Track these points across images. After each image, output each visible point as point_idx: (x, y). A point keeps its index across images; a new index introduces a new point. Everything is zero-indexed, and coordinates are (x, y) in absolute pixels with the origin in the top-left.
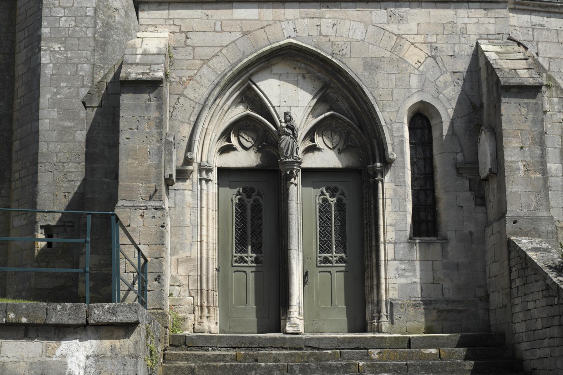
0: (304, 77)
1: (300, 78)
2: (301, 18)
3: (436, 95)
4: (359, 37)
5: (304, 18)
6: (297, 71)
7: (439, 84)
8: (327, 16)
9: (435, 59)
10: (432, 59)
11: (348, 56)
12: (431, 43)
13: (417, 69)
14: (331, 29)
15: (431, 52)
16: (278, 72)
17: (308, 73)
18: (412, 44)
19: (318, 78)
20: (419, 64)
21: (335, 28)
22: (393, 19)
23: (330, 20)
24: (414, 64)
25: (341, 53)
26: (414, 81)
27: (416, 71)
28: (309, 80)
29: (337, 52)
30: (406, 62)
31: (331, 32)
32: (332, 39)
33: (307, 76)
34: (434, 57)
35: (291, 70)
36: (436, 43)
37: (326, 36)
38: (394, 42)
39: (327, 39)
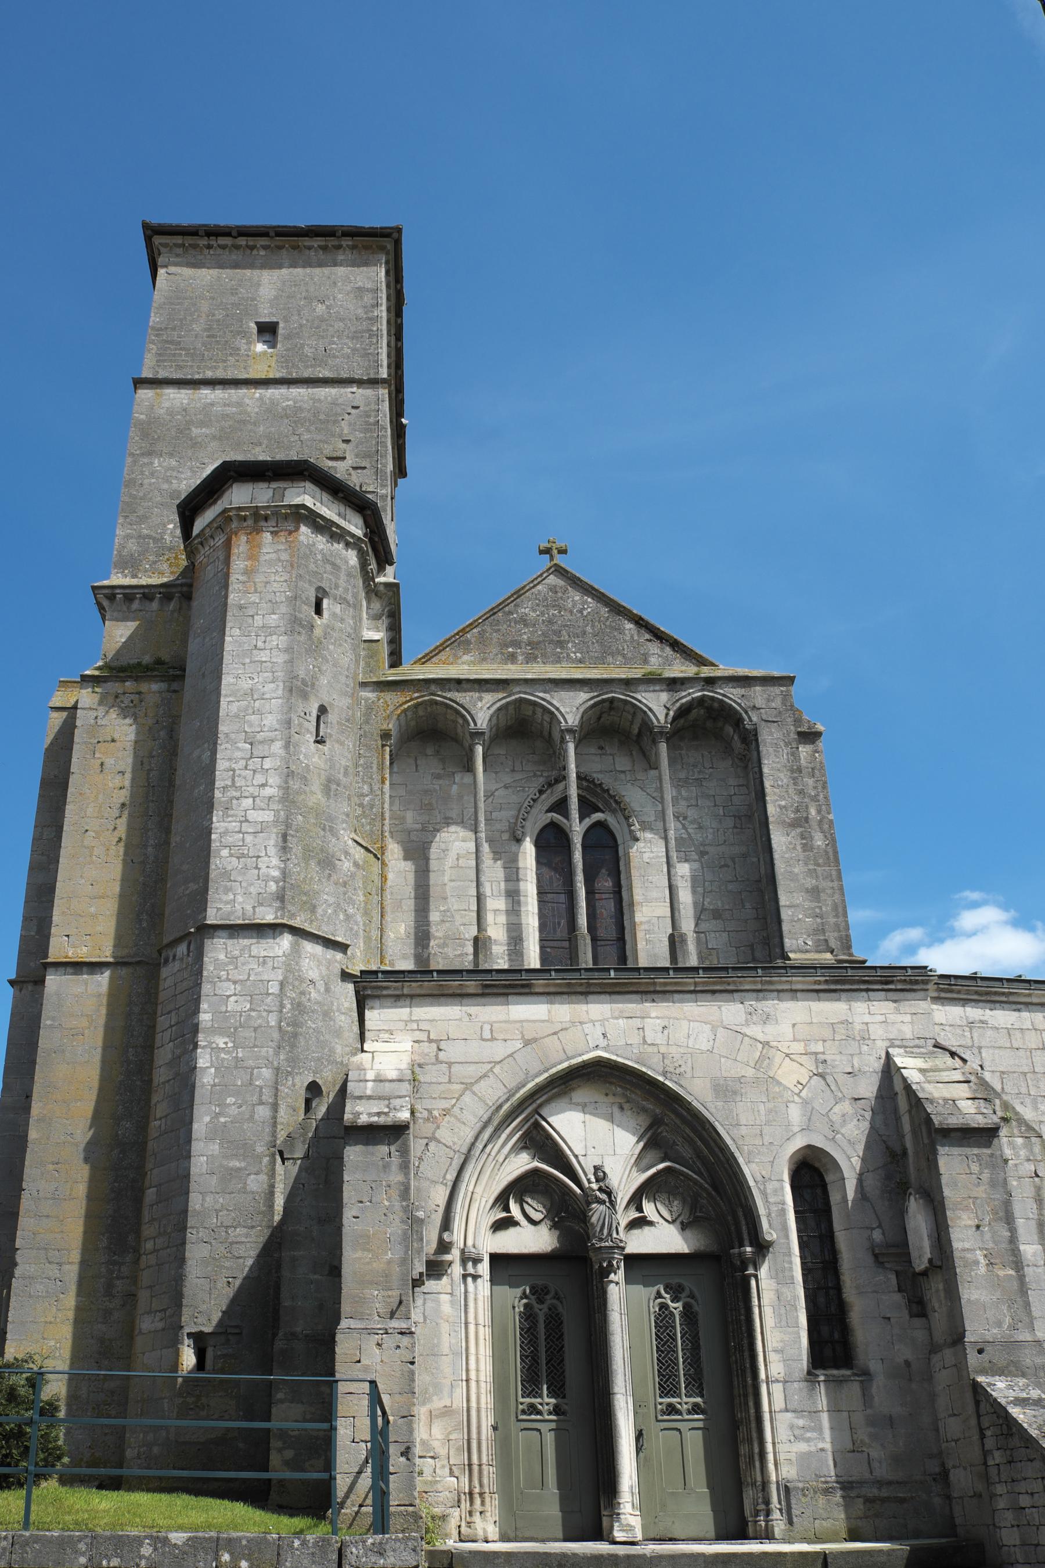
0: (622, 1108)
1: (616, 1110)
2: (613, 1018)
3: (831, 1135)
4: (705, 1046)
5: (617, 1018)
6: (611, 1099)
7: (834, 1118)
8: (653, 1015)
9: (825, 1079)
10: (820, 1079)
11: (689, 1075)
12: (816, 1054)
13: (798, 1095)
14: (660, 1034)
15: (817, 1067)
16: (580, 1101)
17: (628, 1102)
18: (787, 1055)
19: (644, 1110)
20: (801, 1087)
21: (666, 1032)
22: (754, 1017)
23: (658, 1021)
24: (792, 1087)
25: (677, 1072)
26: (795, 1114)
27: (796, 1098)
28: (629, 1113)
29: (672, 1070)
30: (779, 1083)
31: (660, 1039)
32: (663, 1050)
33: (626, 1106)
34: (822, 1076)
35: (601, 1098)
36: (823, 1053)
37: (653, 1044)
38: (759, 1054)
39: (655, 1049)
